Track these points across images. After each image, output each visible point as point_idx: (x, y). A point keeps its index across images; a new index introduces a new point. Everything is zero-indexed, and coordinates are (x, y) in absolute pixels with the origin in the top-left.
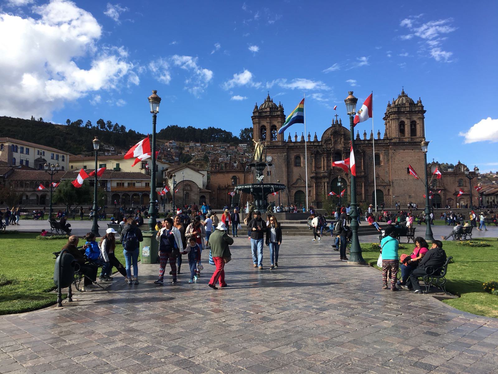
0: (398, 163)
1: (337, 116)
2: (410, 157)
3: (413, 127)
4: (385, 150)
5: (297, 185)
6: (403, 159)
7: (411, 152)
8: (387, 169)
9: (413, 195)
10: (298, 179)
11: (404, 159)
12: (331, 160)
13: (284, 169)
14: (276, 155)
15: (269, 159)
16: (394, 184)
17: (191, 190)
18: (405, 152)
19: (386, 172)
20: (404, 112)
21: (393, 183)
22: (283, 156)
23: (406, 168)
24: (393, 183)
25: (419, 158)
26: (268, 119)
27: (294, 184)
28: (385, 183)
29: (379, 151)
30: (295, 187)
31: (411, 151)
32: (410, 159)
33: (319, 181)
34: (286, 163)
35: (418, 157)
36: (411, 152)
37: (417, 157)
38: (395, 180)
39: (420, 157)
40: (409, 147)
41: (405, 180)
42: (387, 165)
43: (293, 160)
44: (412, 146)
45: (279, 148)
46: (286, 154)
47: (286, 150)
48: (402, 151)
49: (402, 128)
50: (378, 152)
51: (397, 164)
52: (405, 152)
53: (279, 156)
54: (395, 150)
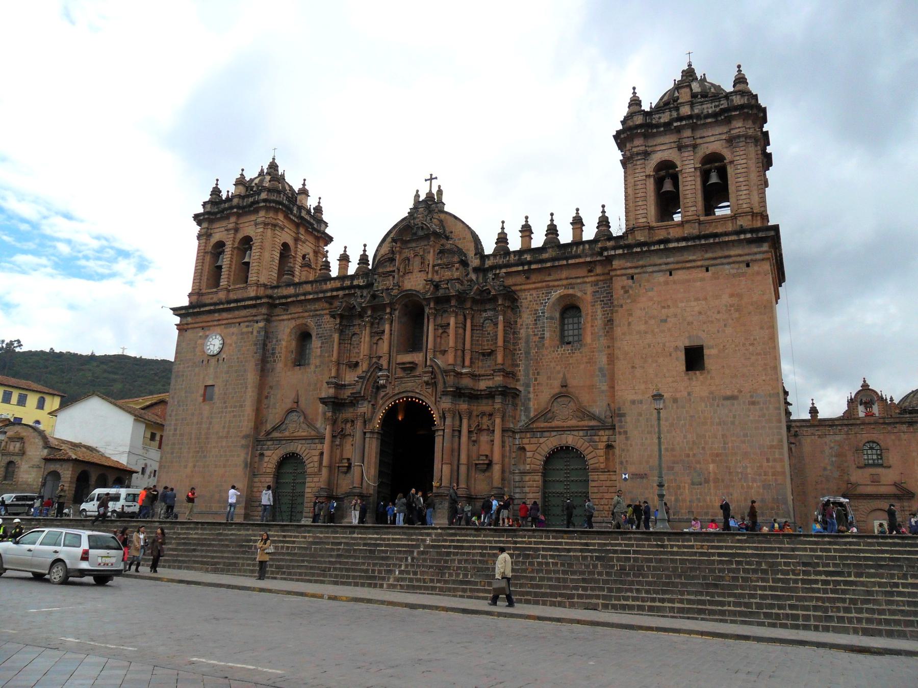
0: (643, 327)
1: (431, 179)
2: (697, 299)
3: (714, 179)
4: (596, 283)
5: (287, 434)
6: (664, 311)
7: (702, 280)
8: (603, 360)
9: (711, 467)
10: (290, 411)
11: (672, 310)
12: (384, 331)
13: (251, 377)
14: (234, 329)
15: (214, 344)
16: (628, 419)
17: (22, 453)
18: (675, 282)
19: (601, 370)
20: (667, 125)
21: (623, 415)
22: (255, 333)
23: (676, 348)
24: (623, 415)
25: (735, 300)
26: (233, 219)
27: (275, 429)
28: (593, 417)
29: (572, 286)
30: (279, 440)
31: (701, 274)
32: (697, 309)
33: (348, 414)
34: (258, 356)
35: (732, 295)
36: (702, 280)
37: (726, 299)
38: (633, 402)
39: (740, 296)
40: (691, 258)
41: (675, 400)
42: (603, 341)
43: (284, 343)
44: (707, 252)
45: (245, 307)
46: (261, 324)
47: (264, 310)
48: (661, 278)
49: (668, 186)
50: (571, 291)
51: (639, 332)
52: (675, 282)
53: (242, 334)
54: (632, 278)
